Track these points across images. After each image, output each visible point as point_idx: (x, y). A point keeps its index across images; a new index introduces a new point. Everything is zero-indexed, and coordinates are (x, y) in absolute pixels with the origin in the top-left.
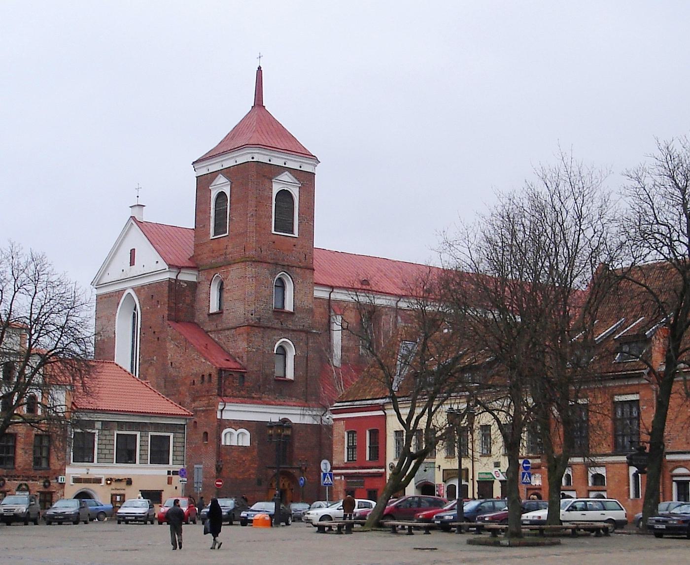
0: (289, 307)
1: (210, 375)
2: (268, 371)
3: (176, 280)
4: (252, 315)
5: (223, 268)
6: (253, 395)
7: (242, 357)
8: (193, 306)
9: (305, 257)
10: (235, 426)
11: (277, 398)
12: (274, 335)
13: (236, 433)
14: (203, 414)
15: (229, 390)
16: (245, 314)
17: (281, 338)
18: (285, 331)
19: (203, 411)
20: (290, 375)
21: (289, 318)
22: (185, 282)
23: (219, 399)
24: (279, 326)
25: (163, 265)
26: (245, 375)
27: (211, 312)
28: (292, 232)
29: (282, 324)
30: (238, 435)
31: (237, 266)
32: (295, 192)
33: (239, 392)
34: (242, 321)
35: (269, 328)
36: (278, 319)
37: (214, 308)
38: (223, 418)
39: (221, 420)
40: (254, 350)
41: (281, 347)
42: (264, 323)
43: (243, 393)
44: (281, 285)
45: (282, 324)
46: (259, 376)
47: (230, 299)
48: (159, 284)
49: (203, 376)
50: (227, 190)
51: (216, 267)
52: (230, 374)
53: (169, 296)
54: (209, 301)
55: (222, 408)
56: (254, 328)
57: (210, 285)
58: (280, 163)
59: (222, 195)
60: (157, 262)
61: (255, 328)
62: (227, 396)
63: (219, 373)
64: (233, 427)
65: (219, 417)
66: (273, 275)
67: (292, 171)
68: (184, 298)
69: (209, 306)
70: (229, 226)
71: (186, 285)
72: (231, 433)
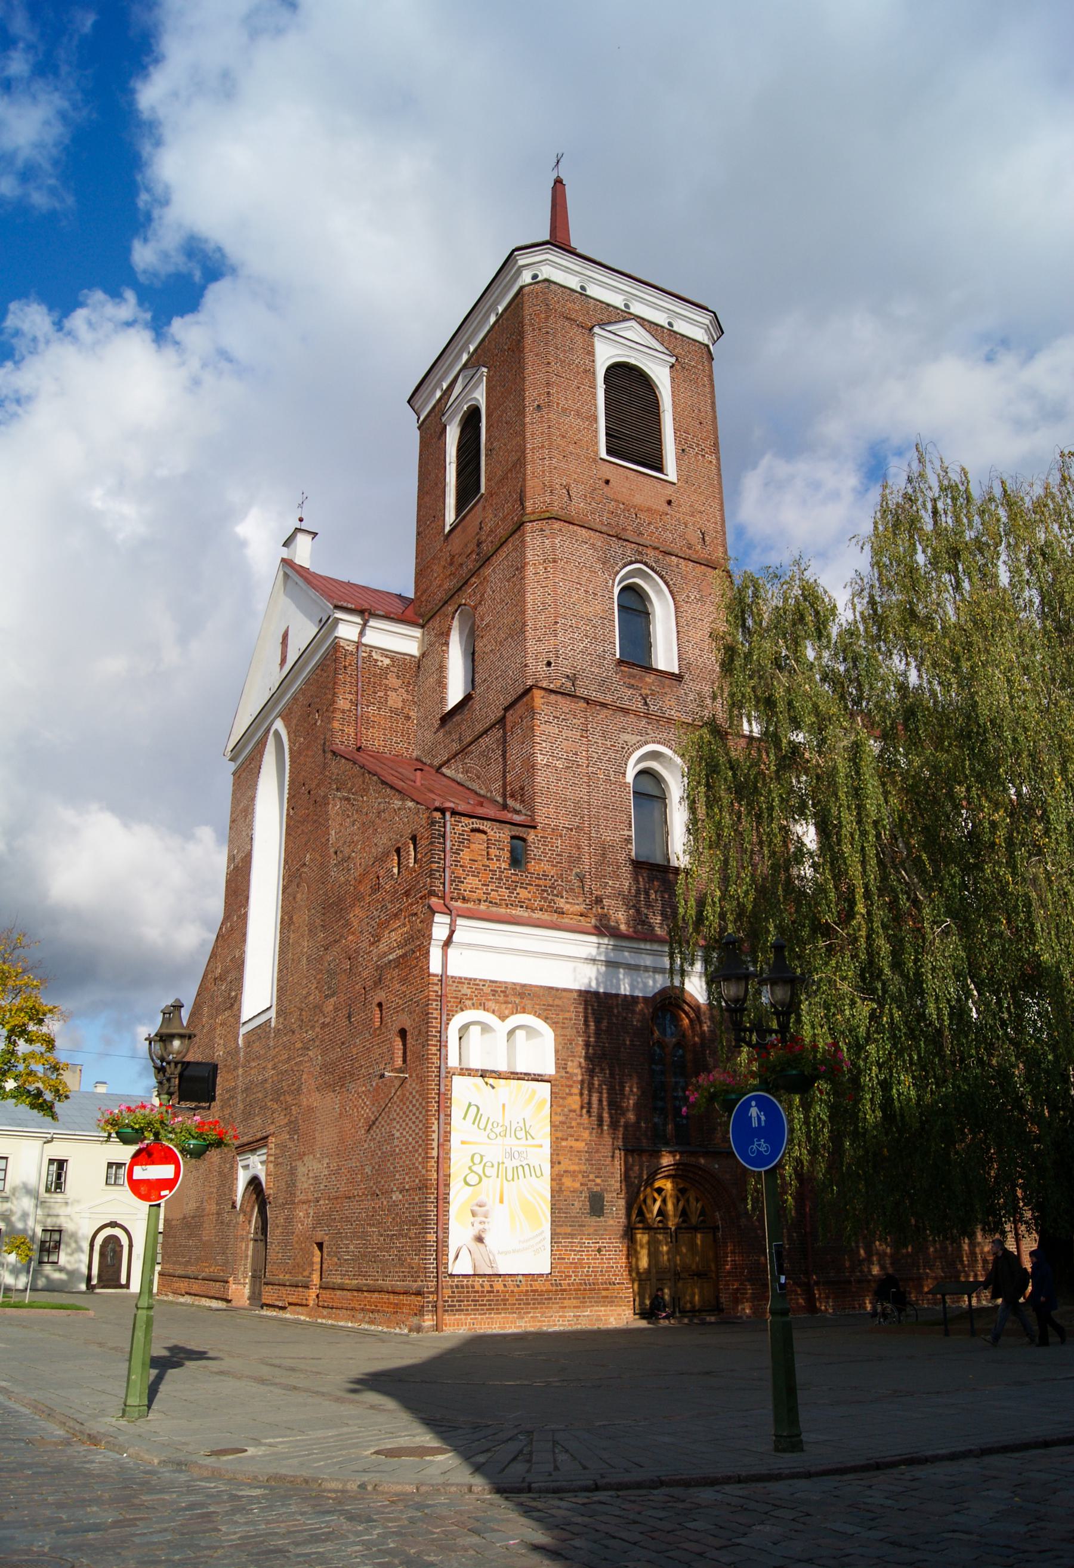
5: (473, 580)
6: (561, 903)
7: (522, 789)
9: (703, 539)
10: (497, 1001)
12: (623, 730)
13: (502, 1028)
15: (472, 882)
18: (658, 721)
21: (667, 690)
22: (385, 652)
26: (531, 836)
28: (660, 469)
29: (646, 704)
32: (661, 375)
33: (511, 889)
35: (604, 705)
36: (631, 686)
38: (451, 972)
39: (443, 978)
40: (559, 764)
43: (524, 894)
45: (646, 704)
47: (488, 649)
55: (444, 937)
56: (553, 697)
58: (617, 300)
59: (472, 417)
61: (559, 698)
64: (491, 1005)
68: (381, 694)
71: (387, 661)
72: (486, 1028)
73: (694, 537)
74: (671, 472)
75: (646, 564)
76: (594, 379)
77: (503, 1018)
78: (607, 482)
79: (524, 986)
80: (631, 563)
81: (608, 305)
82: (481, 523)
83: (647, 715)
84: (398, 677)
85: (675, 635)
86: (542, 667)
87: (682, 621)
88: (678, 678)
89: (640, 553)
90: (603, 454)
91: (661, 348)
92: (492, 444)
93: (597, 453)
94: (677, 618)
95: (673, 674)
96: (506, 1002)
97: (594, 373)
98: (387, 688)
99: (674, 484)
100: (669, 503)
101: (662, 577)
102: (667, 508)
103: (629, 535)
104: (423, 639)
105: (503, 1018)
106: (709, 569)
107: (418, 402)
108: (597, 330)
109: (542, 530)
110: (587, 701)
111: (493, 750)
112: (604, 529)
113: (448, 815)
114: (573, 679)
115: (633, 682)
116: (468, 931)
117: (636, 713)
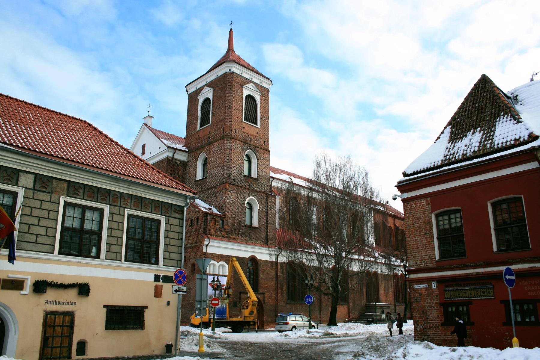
1: (198, 219)
2: (241, 219)
3: (173, 158)
4: (229, 176)
8: (184, 178)
10: (216, 258)
11: (247, 240)
12: (245, 193)
13: (217, 264)
14: (191, 250)
15: (212, 230)
16: (224, 176)
17: (250, 196)
18: (253, 191)
19: (192, 247)
20: (256, 223)
21: (255, 182)
22: (179, 160)
23: (205, 236)
24: (248, 187)
27: (197, 179)
28: (256, 123)
29: (250, 186)
30: (219, 266)
31: (217, 143)
32: (257, 97)
34: (221, 181)
35: (241, 187)
36: (247, 182)
38: (208, 252)
39: (206, 253)
41: (248, 203)
42: (238, 183)
43: (223, 233)
45: (250, 186)
46: (235, 222)
49: (192, 220)
50: (210, 96)
52: (213, 218)
53: (167, 168)
54: (196, 172)
57: (197, 161)
60: (160, 148)
62: (211, 235)
63: (205, 216)
64: (216, 259)
65: (204, 250)
66: (244, 150)
69: (196, 176)
70: (212, 118)
71: (179, 162)
72: (214, 265)
73: (262, 142)
74: (258, 125)
75: (252, 150)
76: (243, 100)
77: (218, 262)
78: (244, 128)
79: (222, 255)
80: (248, 149)
81: (247, 79)
82: (210, 132)
83: (250, 190)
84: (182, 167)
85: (257, 168)
86: (227, 176)
87: (259, 165)
88: (257, 179)
89: (251, 147)
90: (244, 121)
91: (258, 91)
92: (214, 111)
93: (242, 120)
94: (257, 164)
95: (256, 179)
96: (219, 259)
97: (243, 98)
98: (179, 170)
99: (258, 128)
100: (258, 133)
101: (255, 153)
102: (257, 135)
103: (248, 142)
104: (189, 157)
105: (218, 262)
106: (266, 151)
107: (188, 88)
108: (244, 86)
109: (229, 141)
110: (237, 186)
111: (212, 194)
112: (243, 141)
113: (208, 215)
114: (234, 180)
115: (247, 180)
116: (213, 243)
117: (248, 189)
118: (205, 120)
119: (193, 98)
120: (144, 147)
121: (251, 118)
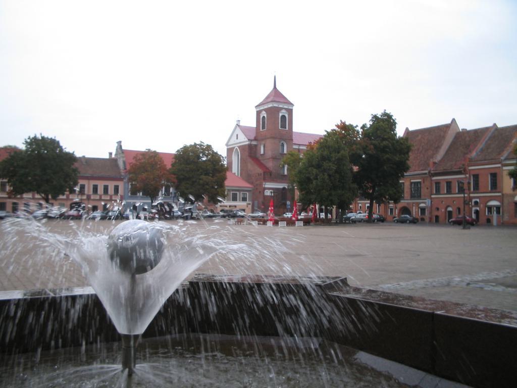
0: (285, 152)
20: (286, 173)
25: (246, 140)
28: (286, 128)
32: (287, 116)
37: (262, 152)
42: (277, 157)
44: (283, 145)
48: (245, 145)
50: (265, 116)
51: (263, 140)
59: (264, 117)
66: (280, 142)
67: (285, 109)
74: (287, 129)
118: (263, 127)
119: (258, 113)
120: (237, 135)
121: (284, 126)
